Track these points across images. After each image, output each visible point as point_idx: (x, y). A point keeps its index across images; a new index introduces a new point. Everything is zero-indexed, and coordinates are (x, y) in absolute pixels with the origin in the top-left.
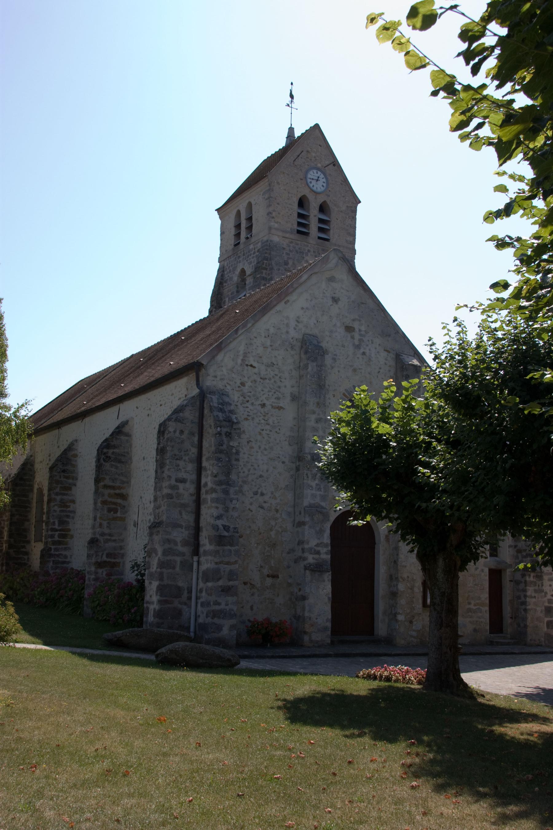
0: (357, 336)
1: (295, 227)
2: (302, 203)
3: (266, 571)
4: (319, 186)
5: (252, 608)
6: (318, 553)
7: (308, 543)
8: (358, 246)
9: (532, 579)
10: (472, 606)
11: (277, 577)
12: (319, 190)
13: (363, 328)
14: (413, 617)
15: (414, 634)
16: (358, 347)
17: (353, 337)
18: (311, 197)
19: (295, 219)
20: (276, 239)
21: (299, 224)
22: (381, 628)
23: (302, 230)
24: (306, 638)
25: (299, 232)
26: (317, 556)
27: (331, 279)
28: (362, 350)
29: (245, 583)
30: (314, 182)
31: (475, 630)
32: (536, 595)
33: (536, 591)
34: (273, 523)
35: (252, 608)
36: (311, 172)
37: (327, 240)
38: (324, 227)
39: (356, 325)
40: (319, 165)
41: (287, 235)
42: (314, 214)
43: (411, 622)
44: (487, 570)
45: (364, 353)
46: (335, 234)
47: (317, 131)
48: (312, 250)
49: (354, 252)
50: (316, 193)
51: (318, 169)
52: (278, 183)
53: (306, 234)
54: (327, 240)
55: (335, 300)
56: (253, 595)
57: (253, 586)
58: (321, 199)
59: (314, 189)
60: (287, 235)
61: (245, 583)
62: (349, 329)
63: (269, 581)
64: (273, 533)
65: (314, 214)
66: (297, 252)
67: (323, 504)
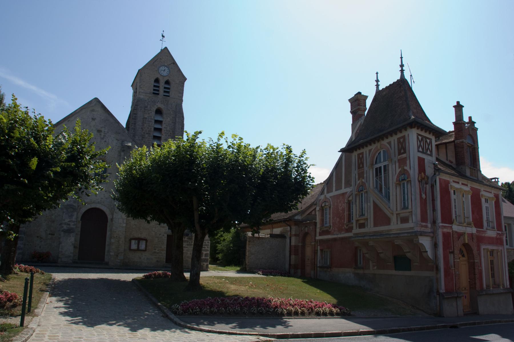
0: (103, 134)
1: (152, 91)
2: (157, 81)
4: (165, 73)
5: (40, 247)
6: (69, 225)
7: (64, 220)
8: (184, 98)
9: (186, 239)
10: (156, 251)
11: (54, 235)
12: (165, 75)
13: (106, 131)
16: (103, 139)
17: (101, 135)
18: (161, 78)
19: (152, 88)
20: (142, 97)
21: (154, 90)
22: (106, 259)
23: (156, 92)
25: (154, 93)
26: (68, 226)
27: (93, 111)
28: (105, 140)
29: (38, 237)
30: (162, 72)
31: (157, 261)
33: (188, 245)
35: (40, 247)
37: (169, 96)
38: (167, 91)
39: (103, 129)
43: (117, 256)
44: (166, 235)
45: (105, 141)
46: (172, 93)
49: (182, 101)
50: (164, 76)
53: (158, 94)
54: (169, 96)
55: (93, 119)
58: (166, 79)
60: (148, 95)
61: (38, 237)
62: (99, 131)
63: (50, 236)
64: (53, 217)
65: (162, 84)
67: (75, 204)
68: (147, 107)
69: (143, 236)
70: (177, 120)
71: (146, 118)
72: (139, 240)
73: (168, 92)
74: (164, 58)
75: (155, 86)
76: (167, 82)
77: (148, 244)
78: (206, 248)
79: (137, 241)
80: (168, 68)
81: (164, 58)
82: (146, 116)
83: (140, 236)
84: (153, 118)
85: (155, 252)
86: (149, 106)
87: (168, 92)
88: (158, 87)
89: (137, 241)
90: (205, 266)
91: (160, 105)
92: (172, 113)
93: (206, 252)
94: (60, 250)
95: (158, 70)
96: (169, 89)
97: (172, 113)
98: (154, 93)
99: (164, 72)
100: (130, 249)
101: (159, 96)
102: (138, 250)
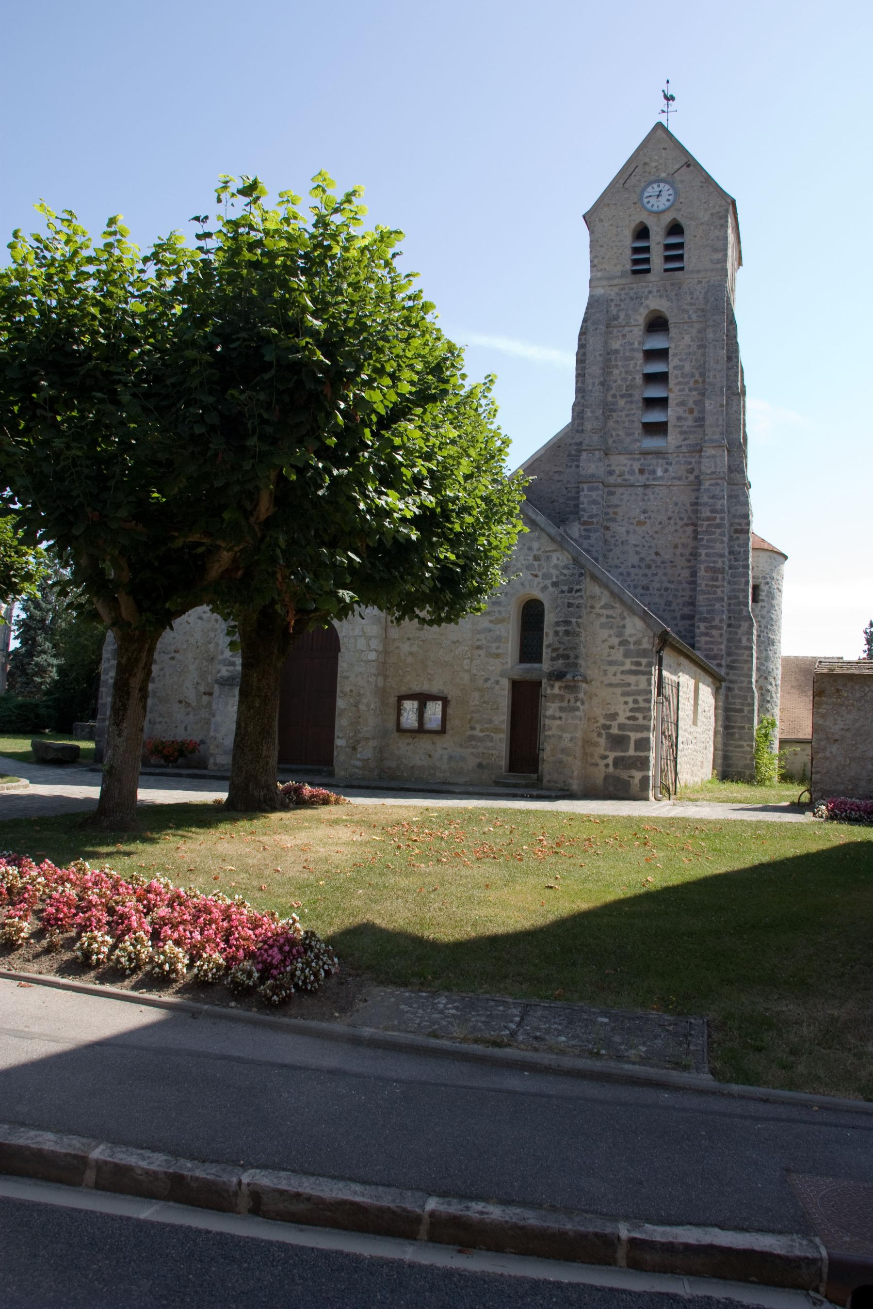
1: (629, 267)
2: (642, 233)
3: (202, 689)
4: (662, 204)
5: (186, 729)
9: (556, 691)
10: (477, 733)
12: (662, 207)
14: (358, 742)
15: (359, 763)
18: (651, 223)
19: (628, 255)
24: (211, 761)
25: (635, 272)
26: (231, 668)
29: (180, 702)
30: (653, 200)
31: (480, 766)
32: (563, 715)
33: (561, 709)
34: (212, 635)
35: (186, 729)
36: (650, 189)
37: (682, 269)
38: (675, 255)
40: (663, 175)
41: (615, 282)
42: (657, 240)
43: (354, 749)
44: (506, 683)
46: (692, 257)
47: (660, 132)
48: (655, 289)
51: (659, 181)
52: (601, 220)
53: (648, 271)
54: (682, 269)
56: (188, 714)
57: (188, 705)
58: (666, 219)
59: (655, 208)
60: (615, 282)
61: (180, 702)
63: (205, 699)
65: (657, 240)
66: (632, 299)
68: (616, 318)
69: (434, 688)
70: (710, 335)
71: (617, 351)
72: (423, 699)
73: (680, 258)
74: (661, 157)
75: (636, 250)
76: (675, 229)
77: (450, 711)
78: (641, 721)
79: (415, 704)
80: (672, 185)
81: (661, 157)
82: (616, 345)
83: (425, 687)
84: (636, 345)
85: (472, 738)
86: (622, 315)
87: (680, 258)
88: (647, 249)
89: (415, 704)
90: (636, 781)
91: (656, 304)
92: (694, 317)
93: (639, 735)
94: (212, 734)
95: (641, 198)
96: (681, 246)
97: (694, 317)
98: (635, 272)
99: (659, 200)
100: (400, 729)
101: (649, 277)
102: (421, 730)
